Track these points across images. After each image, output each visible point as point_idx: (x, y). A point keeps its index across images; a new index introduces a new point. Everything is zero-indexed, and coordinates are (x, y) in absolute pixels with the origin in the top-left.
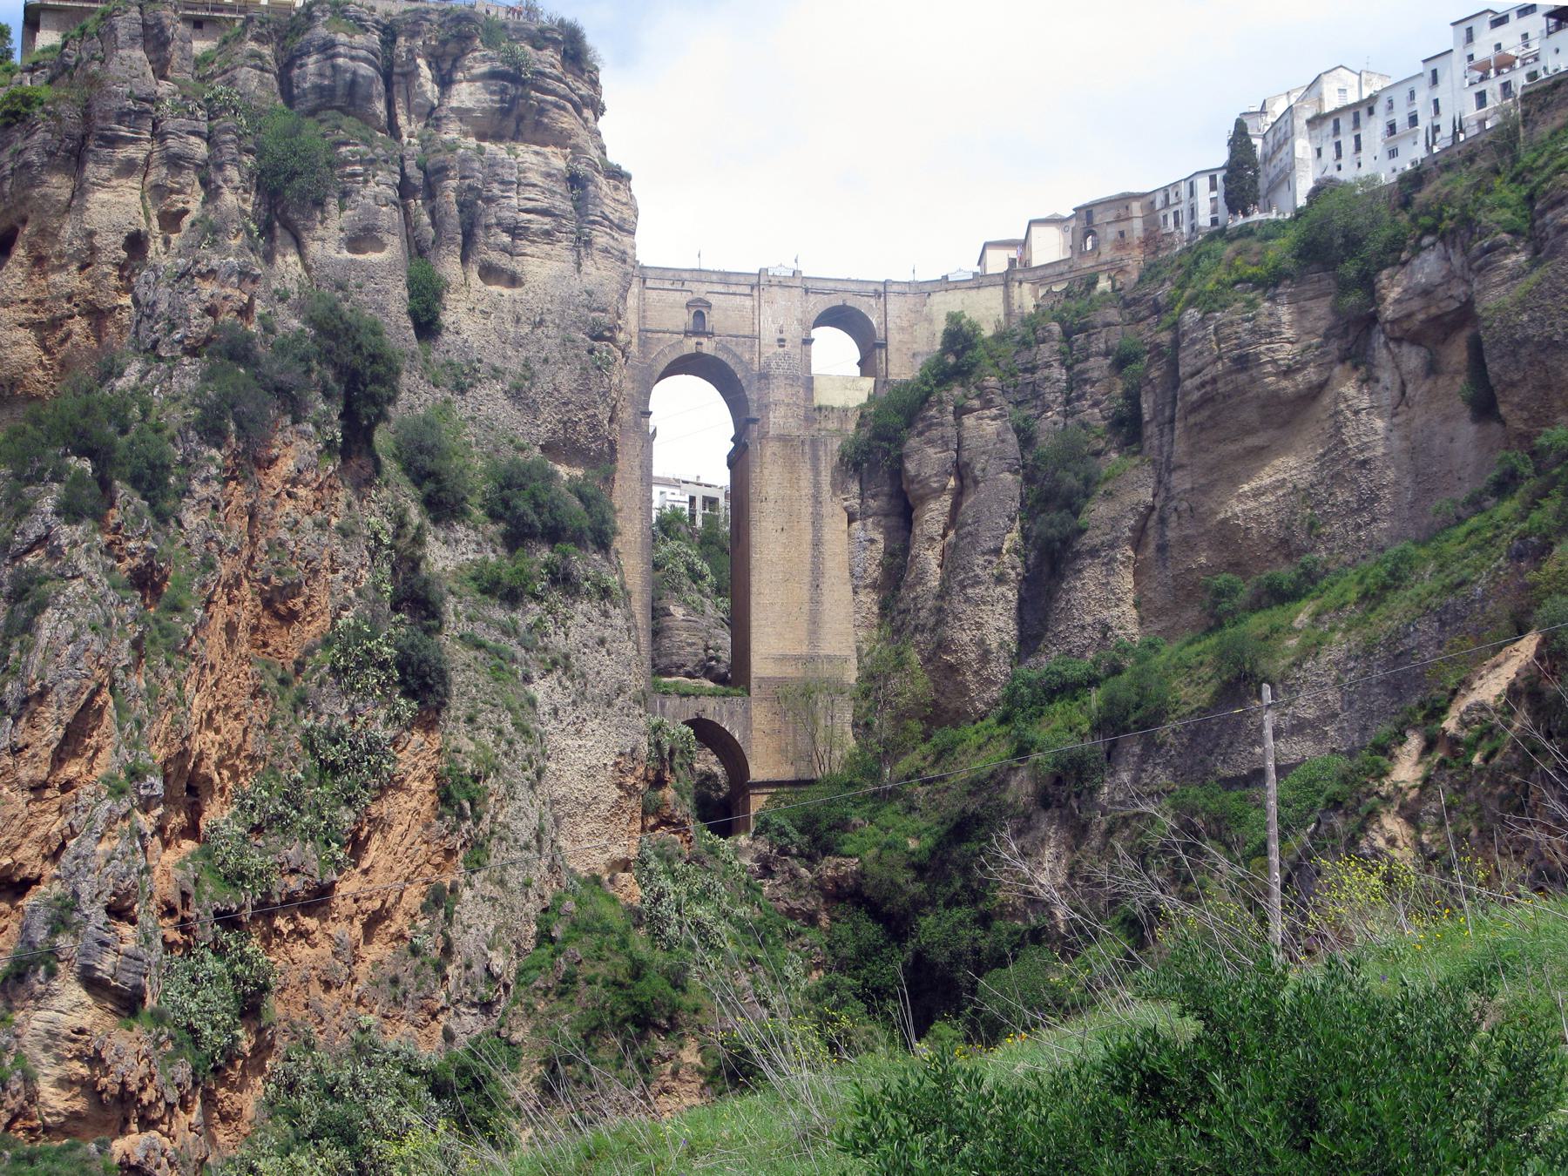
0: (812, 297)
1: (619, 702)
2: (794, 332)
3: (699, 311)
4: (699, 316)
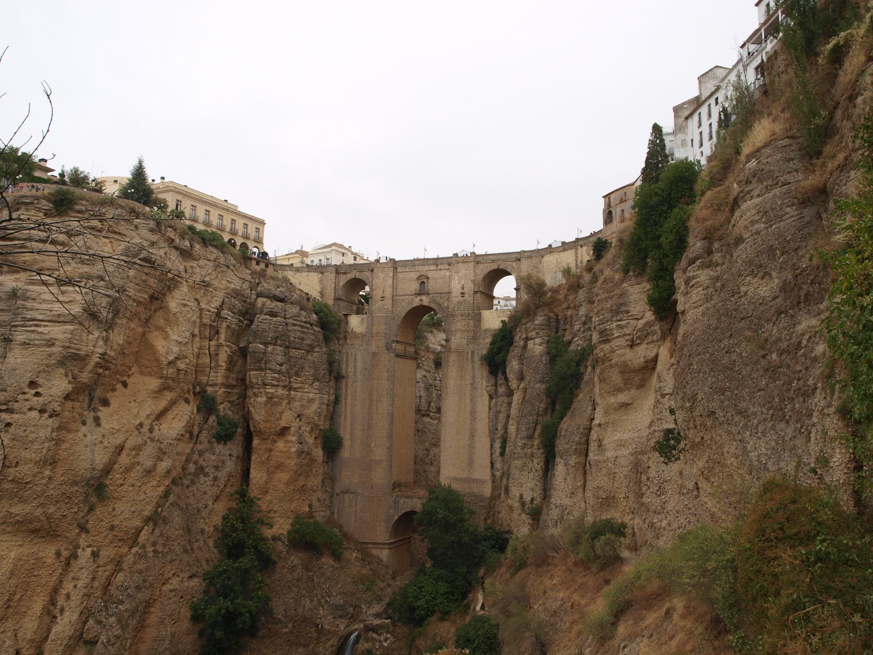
0: (481, 266)
2: (470, 287)
3: (423, 281)
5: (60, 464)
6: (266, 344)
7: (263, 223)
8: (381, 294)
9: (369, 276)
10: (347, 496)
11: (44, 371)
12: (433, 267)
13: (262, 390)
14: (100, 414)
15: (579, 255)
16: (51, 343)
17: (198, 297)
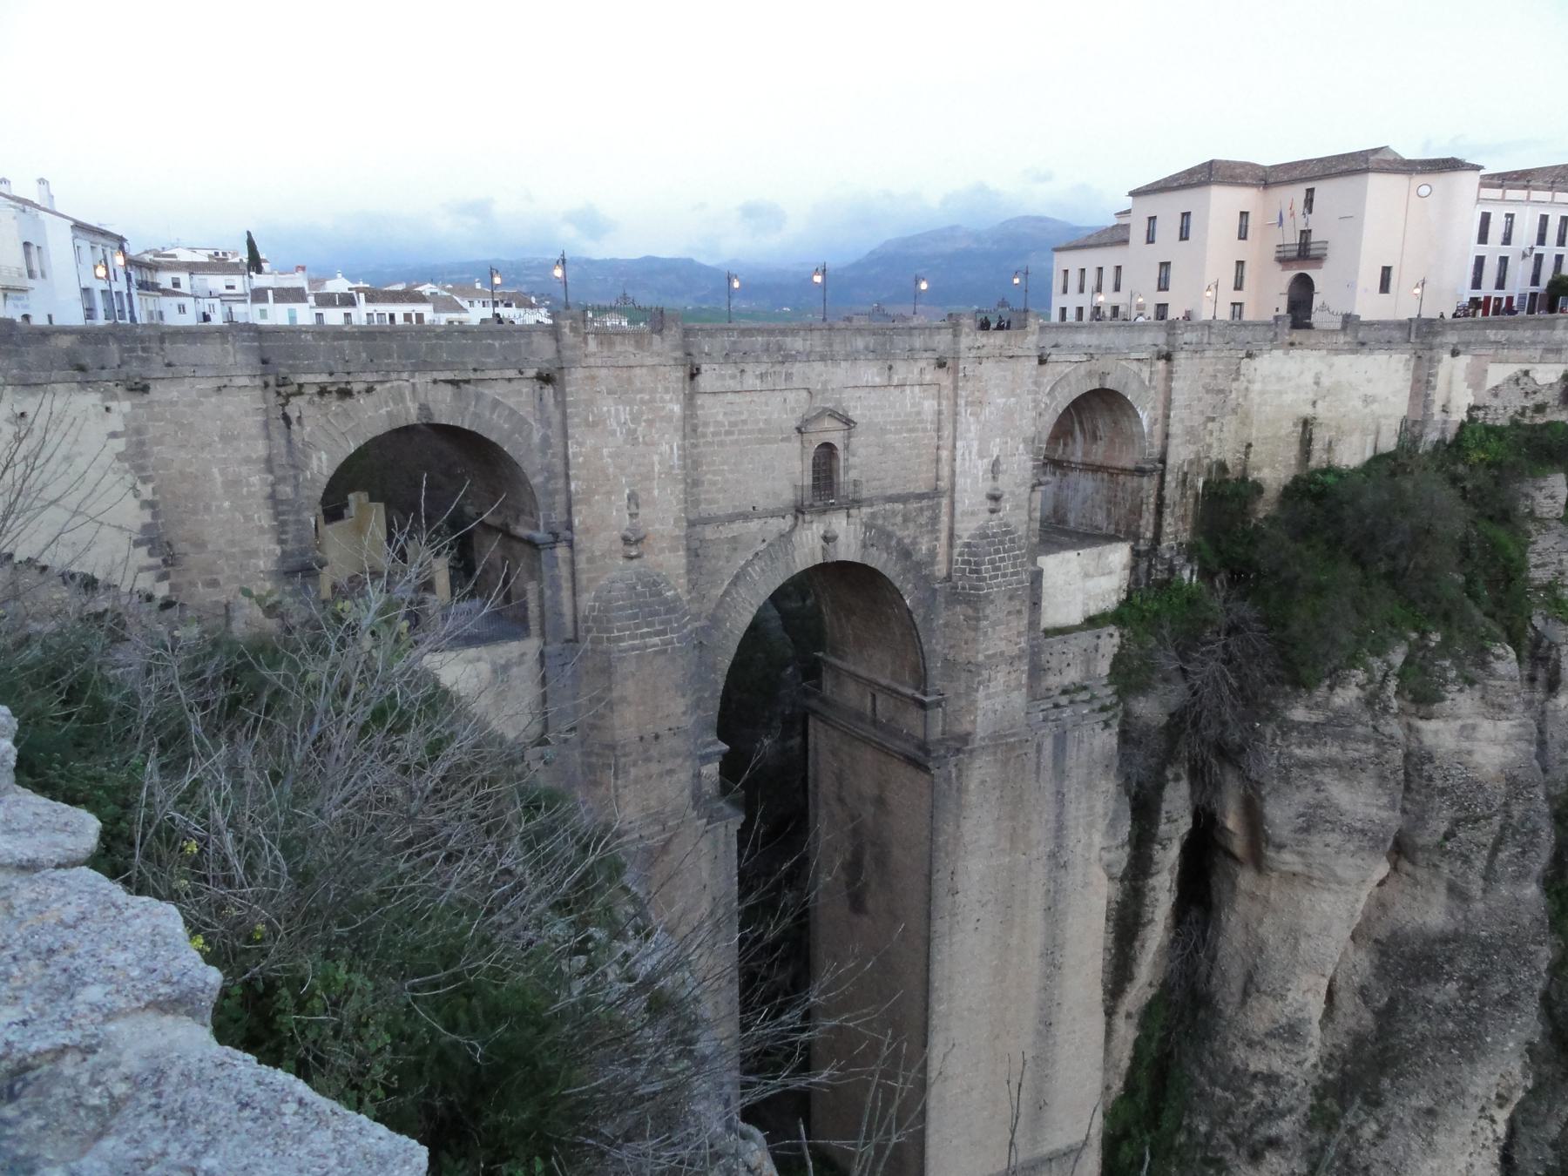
8: (618, 518)
9: (527, 412)
12: (870, 373)
15: (1440, 383)
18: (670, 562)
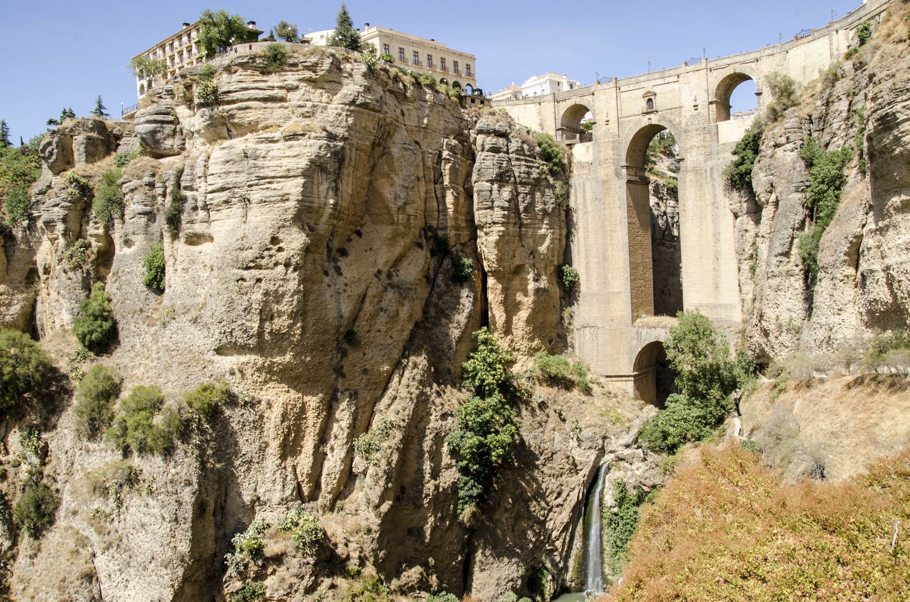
0: (715, 73)
1: (151, 567)
4: (650, 100)
5: (310, 314)
6: (492, 182)
7: (472, 58)
9: (591, 100)
10: (587, 330)
11: (283, 226)
13: (492, 229)
14: (339, 264)
16: (284, 198)
17: (418, 139)
18: (613, 125)
